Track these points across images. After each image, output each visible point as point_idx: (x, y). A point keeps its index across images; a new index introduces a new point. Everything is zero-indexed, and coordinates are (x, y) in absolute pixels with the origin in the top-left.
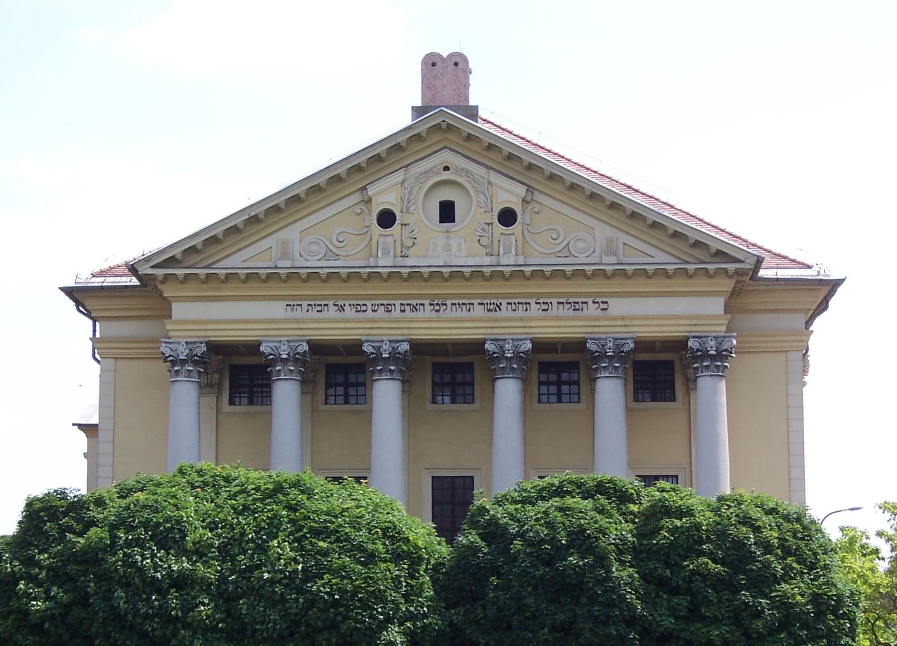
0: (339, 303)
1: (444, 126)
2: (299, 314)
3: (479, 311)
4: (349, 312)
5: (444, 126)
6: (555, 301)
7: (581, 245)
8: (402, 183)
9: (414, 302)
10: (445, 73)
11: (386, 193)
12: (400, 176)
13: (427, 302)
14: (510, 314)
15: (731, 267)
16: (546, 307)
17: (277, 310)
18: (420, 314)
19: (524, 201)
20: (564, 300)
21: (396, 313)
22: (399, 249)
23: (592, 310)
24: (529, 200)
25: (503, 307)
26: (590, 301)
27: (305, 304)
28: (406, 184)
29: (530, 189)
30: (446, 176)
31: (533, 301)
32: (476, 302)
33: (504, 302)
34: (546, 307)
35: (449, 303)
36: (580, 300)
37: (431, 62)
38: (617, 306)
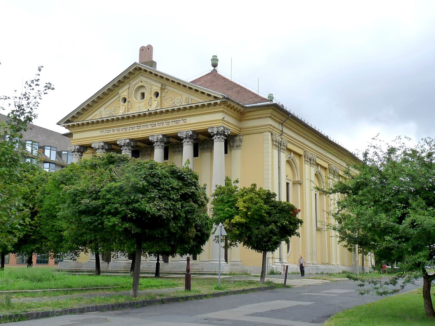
0: (113, 129)
1: (137, 68)
2: (103, 134)
3: (150, 127)
4: (116, 132)
5: (137, 68)
6: (171, 121)
7: (178, 101)
8: (129, 88)
9: (132, 126)
10: (146, 51)
11: (124, 92)
12: (127, 86)
13: (136, 126)
14: (159, 127)
15: (218, 101)
16: (168, 123)
17: (97, 133)
18: (134, 130)
19: (162, 89)
20: (173, 120)
21: (128, 131)
22: (127, 109)
23: (181, 123)
24: (164, 88)
25: (156, 125)
26: (181, 119)
27: (105, 130)
28: (130, 89)
29: (162, 85)
30: (141, 84)
31: (164, 122)
32: (149, 124)
33: (157, 123)
34: (168, 123)
35: (142, 125)
36: (178, 120)
37: (142, 49)
38: (190, 120)
